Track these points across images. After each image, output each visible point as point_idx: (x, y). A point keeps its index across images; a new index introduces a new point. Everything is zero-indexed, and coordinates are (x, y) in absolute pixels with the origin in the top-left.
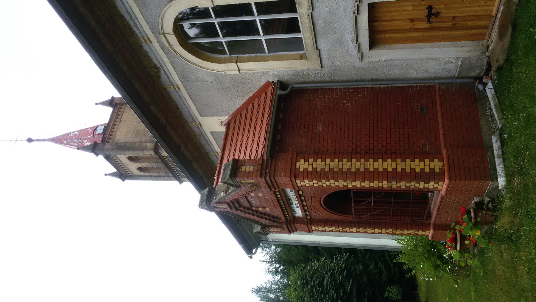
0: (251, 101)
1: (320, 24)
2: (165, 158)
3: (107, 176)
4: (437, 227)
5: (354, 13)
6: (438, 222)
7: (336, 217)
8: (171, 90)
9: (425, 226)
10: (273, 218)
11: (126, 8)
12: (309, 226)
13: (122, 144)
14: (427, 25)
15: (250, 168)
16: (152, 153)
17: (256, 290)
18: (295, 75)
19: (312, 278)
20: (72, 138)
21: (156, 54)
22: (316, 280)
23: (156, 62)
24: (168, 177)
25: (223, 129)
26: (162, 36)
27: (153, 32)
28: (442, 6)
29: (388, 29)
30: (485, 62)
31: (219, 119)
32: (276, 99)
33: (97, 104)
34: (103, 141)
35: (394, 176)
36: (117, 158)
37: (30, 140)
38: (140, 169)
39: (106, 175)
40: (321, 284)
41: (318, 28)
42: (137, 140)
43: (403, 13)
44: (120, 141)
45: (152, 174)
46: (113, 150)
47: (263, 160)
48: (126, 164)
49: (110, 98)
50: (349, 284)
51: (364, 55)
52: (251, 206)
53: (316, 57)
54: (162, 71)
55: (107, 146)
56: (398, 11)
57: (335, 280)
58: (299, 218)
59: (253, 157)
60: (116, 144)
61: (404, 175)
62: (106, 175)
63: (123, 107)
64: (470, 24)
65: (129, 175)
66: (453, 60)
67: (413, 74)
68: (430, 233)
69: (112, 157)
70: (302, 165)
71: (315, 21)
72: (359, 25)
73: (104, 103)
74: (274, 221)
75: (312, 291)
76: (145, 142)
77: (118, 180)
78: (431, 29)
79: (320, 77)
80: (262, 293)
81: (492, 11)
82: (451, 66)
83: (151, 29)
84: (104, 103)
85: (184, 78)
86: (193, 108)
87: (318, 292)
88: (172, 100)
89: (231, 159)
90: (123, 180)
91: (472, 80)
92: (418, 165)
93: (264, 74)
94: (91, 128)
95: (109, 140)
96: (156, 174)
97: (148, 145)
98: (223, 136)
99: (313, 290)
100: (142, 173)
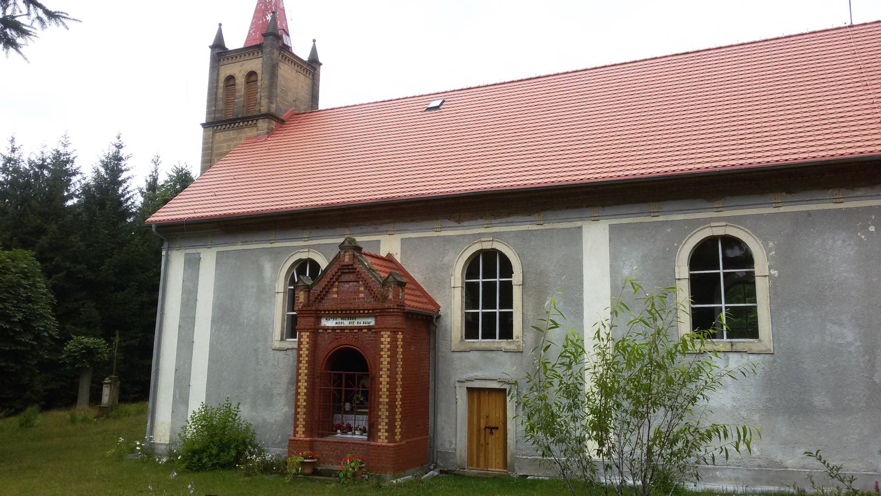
0: (422, 290)
1: (494, 355)
2: (255, 121)
3: (218, 26)
5: (500, 379)
7: (322, 355)
8: (436, 225)
10: (321, 298)
11: (516, 222)
12: (310, 330)
13: (276, 72)
14: (483, 426)
16: (264, 109)
18: (446, 330)
21: (474, 227)
23: (466, 223)
24: (215, 112)
25: (383, 253)
26: (492, 239)
27: (494, 233)
28: (497, 436)
29: (482, 401)
30: (451, 469)
31: (397, 254)
33: (314, 41)
36: (254, 57)
38: (230, 78)
39: (220, 25)
40: (29, 300)
41: (489, 354)
43: (494, 411)
44: (279, 69)
45: (220, 91)
47: (404, 306)
48: (243, 64)
49: (320, 61)
50: (30, 340)
51: (462, 383)
52: (339, 282)
53: (463, 348)
54: (455, 224)
55: (276, 52)
56: (496, 407)
60: (277, 63)
62: (220, 25)
63: (311, 77)
64: (482, 455)
65: (222, 60)
66: (453, 446)
67: (441, 419)
69: (258, 52)
70: (400, 336)
71: (494, 352)
72: (490, 382)
73: (314, 52)
74: (316, 298)
78: (479, 430)
79: (442, 348)
81: (491, 468)
82: (447, 445)
83: (497, 232)
84: (314, 52)
85: (448, 239)
88: (423, 220)
90: (213, 47)
91: (435, 461)
93: (449, 305)
95: (281, 56)
100: (222, 77)
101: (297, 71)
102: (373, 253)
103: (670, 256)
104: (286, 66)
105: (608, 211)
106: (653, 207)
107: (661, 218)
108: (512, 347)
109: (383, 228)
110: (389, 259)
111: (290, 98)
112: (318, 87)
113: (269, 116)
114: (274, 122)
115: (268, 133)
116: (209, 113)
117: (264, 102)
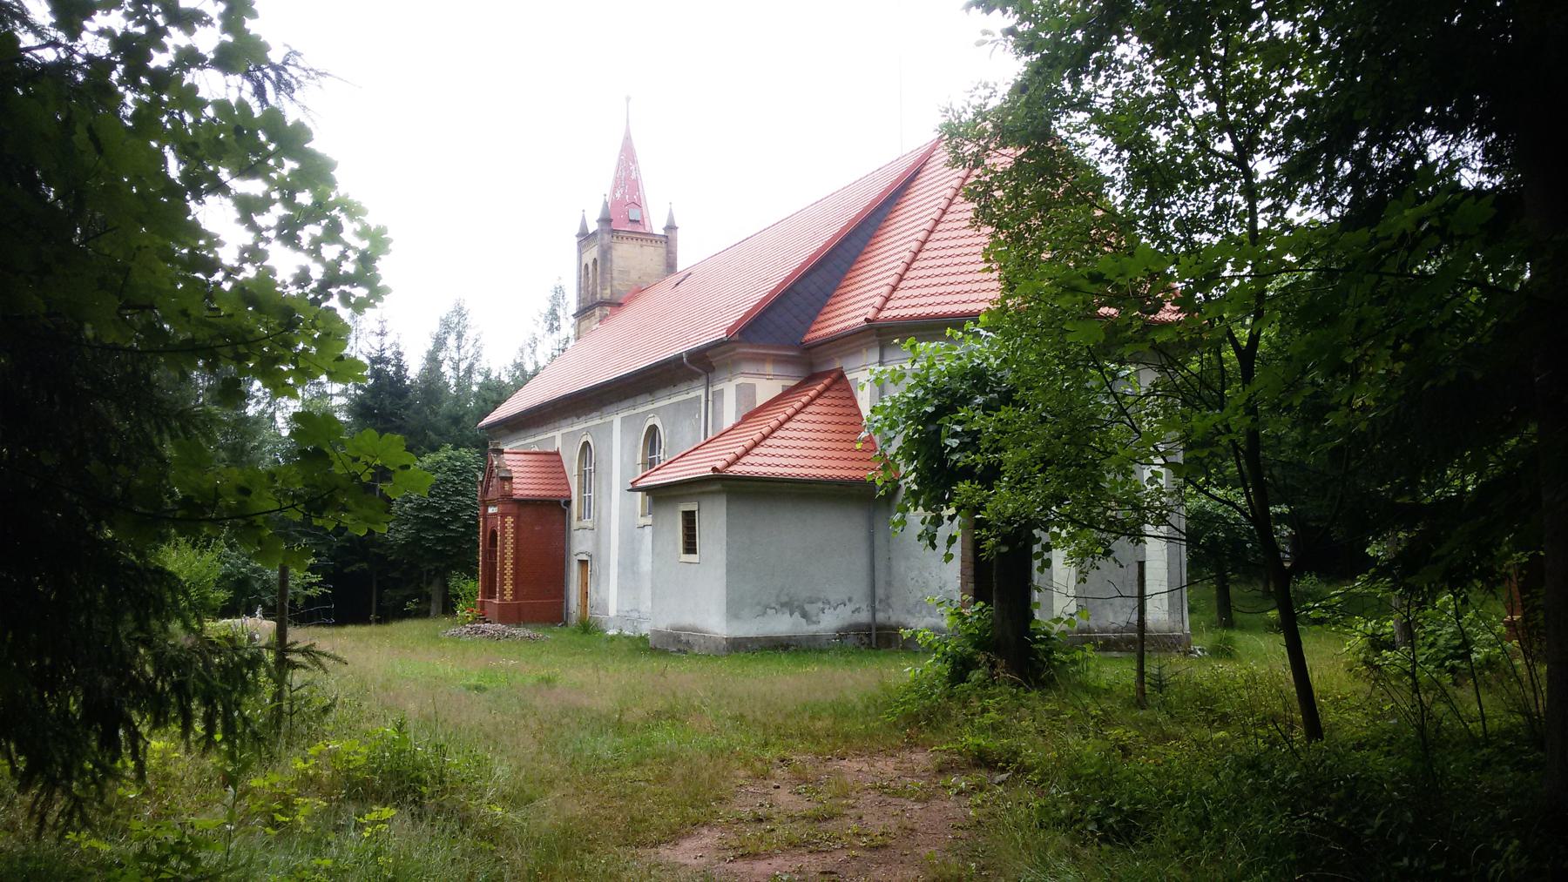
4: (483, 603)
6: (486, 605)
8: (569, 421)
15: (507, 488)
17: (461, 309)
20: (627, 169)
22: (463, 486)
32: (557, 499)
37: (628, 99)
38: (586, 265)
40: (457, 492)
44: (614, 253)
46: (602, 246)
55: (607, 237)
57: (463, 510)
58: (487, 510)
59: (514, 486)
60: (610, 248)
61: (503, 580)
70: (509, 520)
75: (448, 481)
76: (611, 286)
77: (577, 231)
80: (456, 321)
89: (514, 475)
90: (577, 236)
92: (509, 588)
96: (582, 285)
97: (608, 291)
98: (549, 450)
101: (642, 246)
104: (625, 246)
106: (630, 402)
107: (636, 411)
108: (591, 526)
109: (557, 425)
110: (557, 453)
111: (634, 276)
113: (602, 304)
114: (609, 309)
116: (580, 302)
117: (598, 289)
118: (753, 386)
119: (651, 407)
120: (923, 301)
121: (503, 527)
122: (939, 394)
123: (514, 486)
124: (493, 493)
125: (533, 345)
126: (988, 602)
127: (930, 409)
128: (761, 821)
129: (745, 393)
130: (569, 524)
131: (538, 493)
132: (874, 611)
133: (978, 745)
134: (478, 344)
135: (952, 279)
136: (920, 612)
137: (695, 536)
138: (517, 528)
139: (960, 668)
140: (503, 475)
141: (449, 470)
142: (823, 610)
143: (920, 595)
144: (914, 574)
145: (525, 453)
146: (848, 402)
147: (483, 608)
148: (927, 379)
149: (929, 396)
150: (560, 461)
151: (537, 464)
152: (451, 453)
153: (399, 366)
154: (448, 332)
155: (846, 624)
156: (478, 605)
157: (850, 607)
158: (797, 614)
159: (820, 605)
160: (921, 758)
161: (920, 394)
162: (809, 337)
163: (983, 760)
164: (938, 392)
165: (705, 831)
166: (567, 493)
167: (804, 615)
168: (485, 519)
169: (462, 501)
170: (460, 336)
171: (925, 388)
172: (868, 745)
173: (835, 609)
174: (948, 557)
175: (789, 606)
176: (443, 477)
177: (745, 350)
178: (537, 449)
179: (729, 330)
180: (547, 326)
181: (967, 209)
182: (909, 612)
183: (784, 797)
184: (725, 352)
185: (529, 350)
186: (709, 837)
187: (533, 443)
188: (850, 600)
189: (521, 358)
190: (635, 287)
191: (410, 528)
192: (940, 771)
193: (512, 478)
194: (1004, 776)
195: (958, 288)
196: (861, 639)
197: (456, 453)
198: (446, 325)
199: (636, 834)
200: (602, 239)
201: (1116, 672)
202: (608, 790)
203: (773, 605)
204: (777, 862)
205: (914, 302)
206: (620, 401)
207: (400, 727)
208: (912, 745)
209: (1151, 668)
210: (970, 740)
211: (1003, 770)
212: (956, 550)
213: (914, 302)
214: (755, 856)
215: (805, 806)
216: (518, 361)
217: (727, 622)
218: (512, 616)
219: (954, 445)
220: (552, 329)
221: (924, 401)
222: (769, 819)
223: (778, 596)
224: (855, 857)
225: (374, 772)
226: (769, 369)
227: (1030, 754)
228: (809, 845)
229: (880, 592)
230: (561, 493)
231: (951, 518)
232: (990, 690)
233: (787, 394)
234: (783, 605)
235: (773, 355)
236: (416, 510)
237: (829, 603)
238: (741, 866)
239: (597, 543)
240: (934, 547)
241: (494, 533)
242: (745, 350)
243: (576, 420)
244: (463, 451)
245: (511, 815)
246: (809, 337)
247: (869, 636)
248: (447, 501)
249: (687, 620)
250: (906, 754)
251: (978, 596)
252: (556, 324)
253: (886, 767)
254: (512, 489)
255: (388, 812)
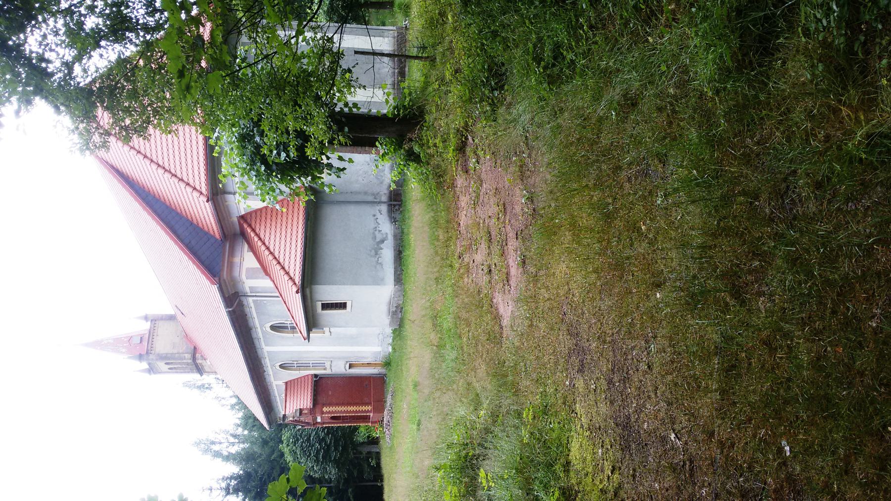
6: (373, 420)
8: (267, 377)
9: (368, 422)
15: (306, 412)
19: (301, 437)
34: (147, 353)
35: (357, 412)
38: (169, 369)
42: (175, 351)
46: (157, 360)
49: (144, 314)
55: (151, 357)
57: (319, 436)
60: (158, 354)
61: (359, 411)
63: (157, 322)
68: (370, 424)
70: (325, 409)
73: (140, 318)
75: (302, 446)
77: (147, 375)
80: (203, 445)
84: (140, 318)
86: (272, 379)
87: (307, 446)
89: (298, 408)
90: (150, 374)
94: (127, 337)
97: (186, 355)
98: (284, 387)
99: (302, 444)
101: (157, 335)
102: (284, 392)
103: (283, 337)
105: (258, 346)
106: (256, 342)
107: (261, 337)
108: (329, 363)
110: (286, 383)
112: (162, 316)
113: (194, 358)
114: (197, 355)
115: (205, 360)
117: (184, 361)
118: (248, 270)
119: (259, 330)
120: (196, 168)
121: (329, 412)
122: (254, 162)
123: (305, 407)
124: (309, 419)
125: (220, 399)
126: (376, 139)
127: (263, 168)
128: (490, 271)
129: (251, 274)
130: (328, 375)
131: (309, 393)
132: (380, 202)
133: (453, 150)
134: (218, 432)
135: (182, 149)
136: (382, 176)
137: (336, 303)
138: (330, 405)
139: (412, 157)
140: (298, 414)
141: (295, 445)
142: (380, 231)
143: (372, 176)
144: (360, 179)
145: (286, 402)
146: (258, 214)
147: (375, 422)
148: (245, 169)
149: (255, 168)
150: (290, 381)
151: (292, 395)
152: (285, 445)
153: (231, 478)
154: (211, 450)
155: (387, 218)
156: (373, 425)
157: (378, 215)
158: (382, 246)
159: (377, 233)
160: (460, 181)
161: (254, 173)
162: (217, 236)
163: (461, 148)
164: (252, 163)
165: (495, 301)
166: (310, 377)
167: (382, 241)
168: (324, 423)
169: (314, 437)
170: (213, 443)
171: (250, 170)
172: (453, 211)
173: (379, 224)
174: (351, 161)
175: (377, 250)
176: (298, 448)
177: (225, 273)
178: (284, 395)
179: (213, 283)
180: (208, 391)
181: (136, 141)
182: (382, 183)
183: (479, 257)
184: (226, 286)
185: (223, 402)
186: (498, 299)
187: (280, 397)
188: (374, 216)
189: (227, 405)
190: (184, 339)
191: (329, 466)
192: (467, 172)
193: (300, 409)
194: (470, 137)
195: (188, 146)
196: (396, 210)
197: (285, 442)
198: (207, 451)
199: (496, 338)
200: (153, 359)
201: (416, 71)
202: (473, 353)
203: (376, 259)
204: (511, 263)
205: (196, 173)
206: (255, 347)
207: (438, 469)
208: (453, 186)
209: (414, 52)
210: (450, 155)
211: (467, 138)
212: (346, 156)
213: (196, 173)
214: (508, 274)
215: (484, 246)
216: (229, 407)
217: (384, 285)
218: (380, 406)
219: (285, 155)
220: (209, 388)
221: (258, 171)
222: (489, 266)
223: (371, 256)
224: (510, 221)
225: (461, 482)
226: (237, 260)
227: (459, 123)
228: (504, 244)
229: (370, 198)
230: (310, 380)
231: (328, 158)
232: (425, 141)
233: (252, 249)
234: (376, 254)
235: (228, 257)
236: (318, 463)
237: (376, 227)
238: (513, 282)
239: (339, 358)
240: (344, 169)
241: (333, 418)
242: (225, 273)
243: (266, 373)
244: (284, 438)
245: (485, 406)
246: (217, 236)
247: (395, 206)
248: (313, 445)
249: (384, 308)
250: (457, 189)
251: (374, 146)
252: (207, 386)
253: (464, 201)
254: (307, 409)
255: (482, 473)
